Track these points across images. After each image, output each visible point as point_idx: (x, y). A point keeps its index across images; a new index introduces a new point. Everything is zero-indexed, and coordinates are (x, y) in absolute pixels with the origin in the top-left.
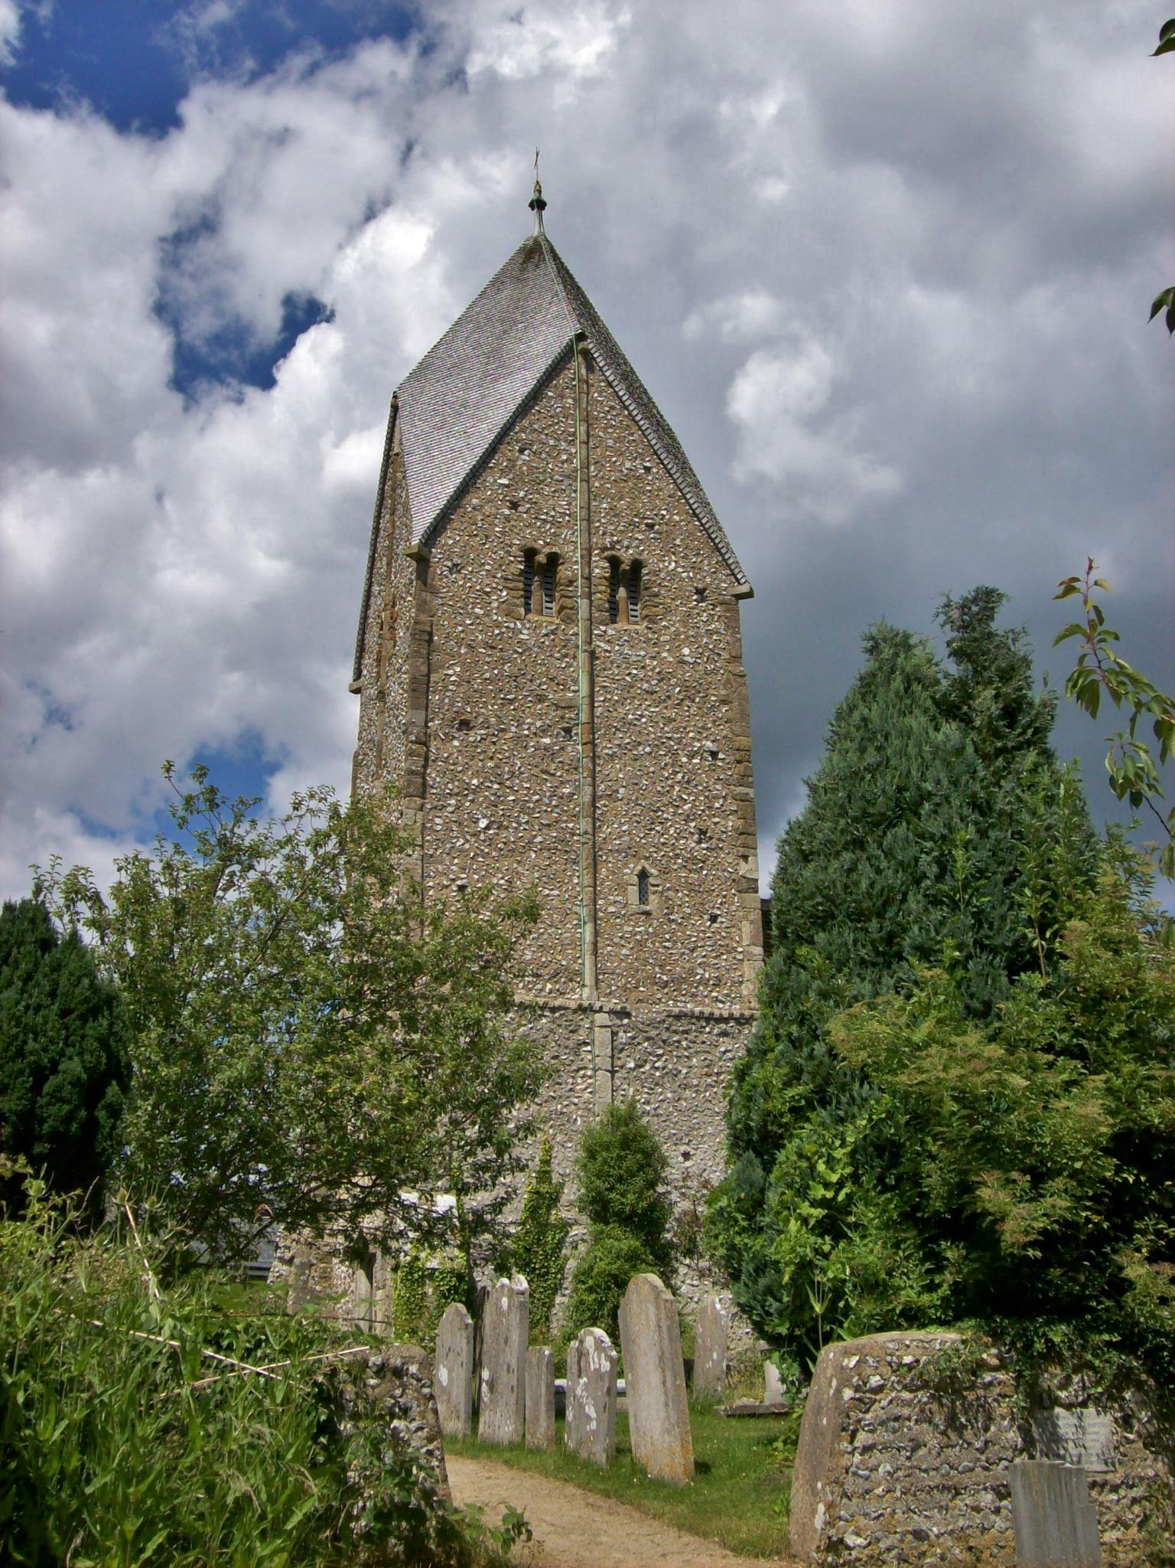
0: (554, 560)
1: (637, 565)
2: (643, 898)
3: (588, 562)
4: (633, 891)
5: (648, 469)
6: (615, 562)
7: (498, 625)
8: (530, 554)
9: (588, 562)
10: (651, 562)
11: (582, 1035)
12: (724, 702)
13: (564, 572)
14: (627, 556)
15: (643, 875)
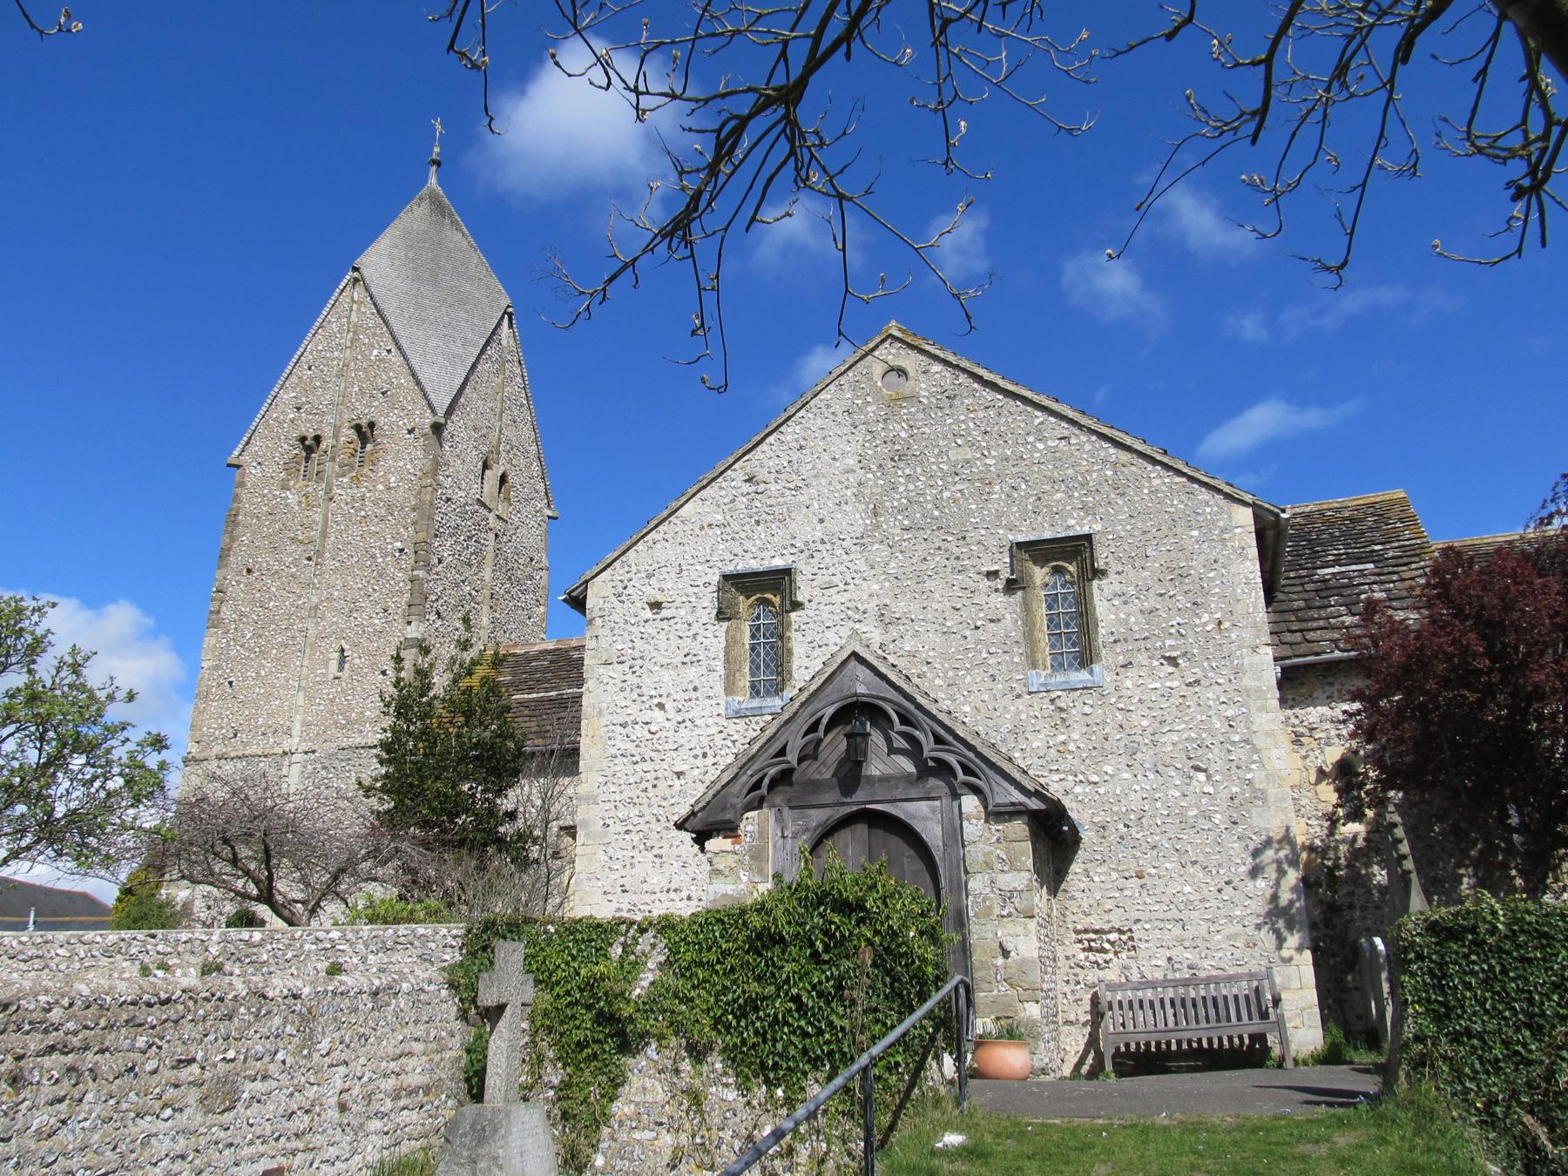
0: (318, 439)
1: (372, 425)
2: (341, 668)
3: (336, 436)
4: (334, 665)
5: (389, 351)
6: (358, 428)
7: (275, 497)
8: (303, 439)
9: (336, 436)
10: (381, 421)
11: (284, 772)
12: (414, 510)
13: (323, 446)
14: (364, 422)
15: (343, 650)
